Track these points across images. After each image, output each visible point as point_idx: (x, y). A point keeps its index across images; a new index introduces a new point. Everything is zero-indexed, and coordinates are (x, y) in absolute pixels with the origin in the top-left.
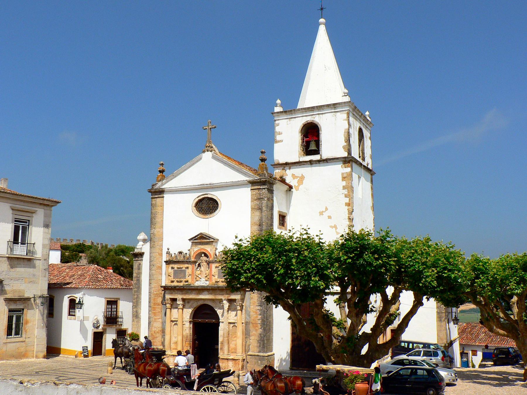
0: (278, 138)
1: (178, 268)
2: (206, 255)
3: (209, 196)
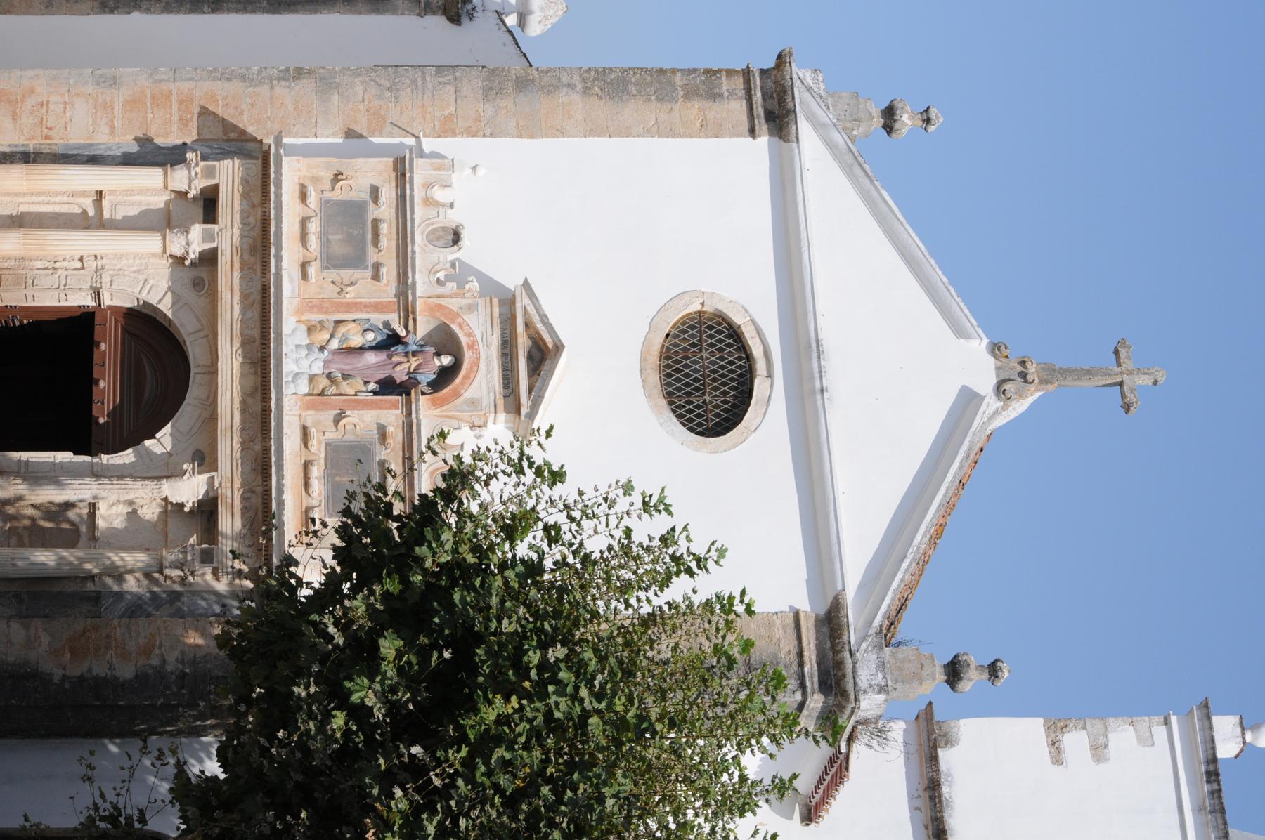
0: (1076, 741)
1: (376, 222)
3: (760, 387)
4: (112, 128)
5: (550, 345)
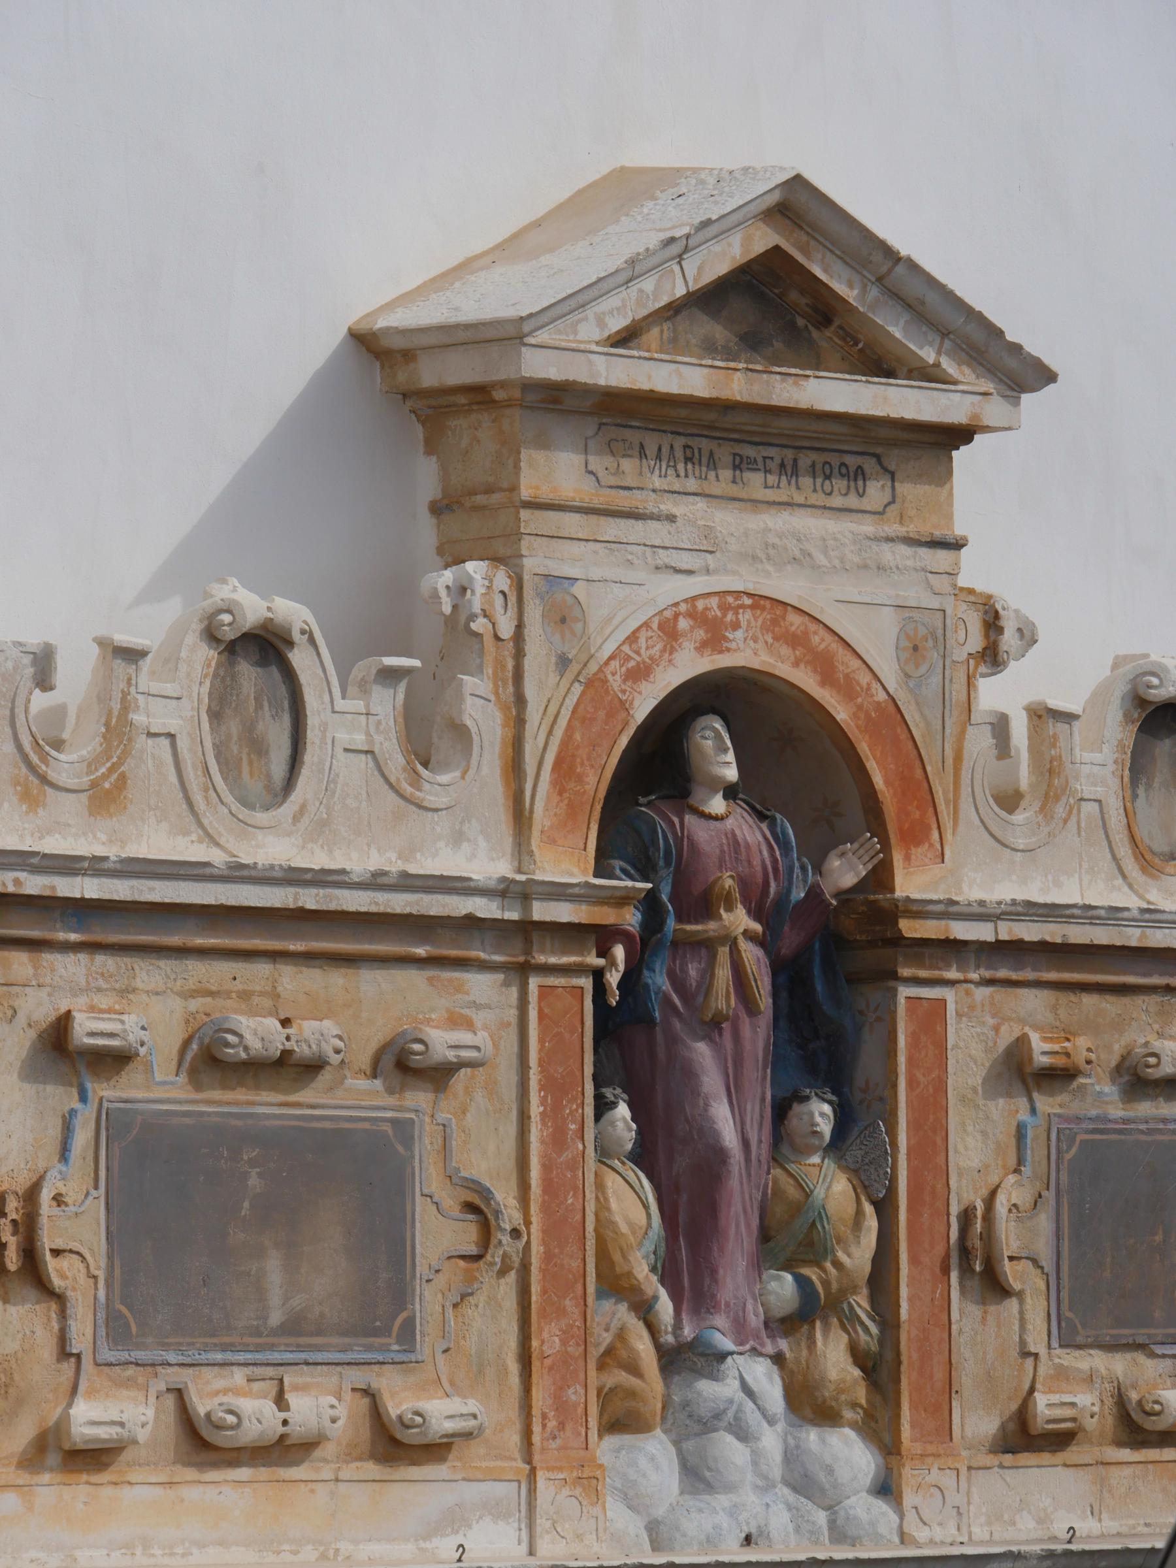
5: (764, 239)
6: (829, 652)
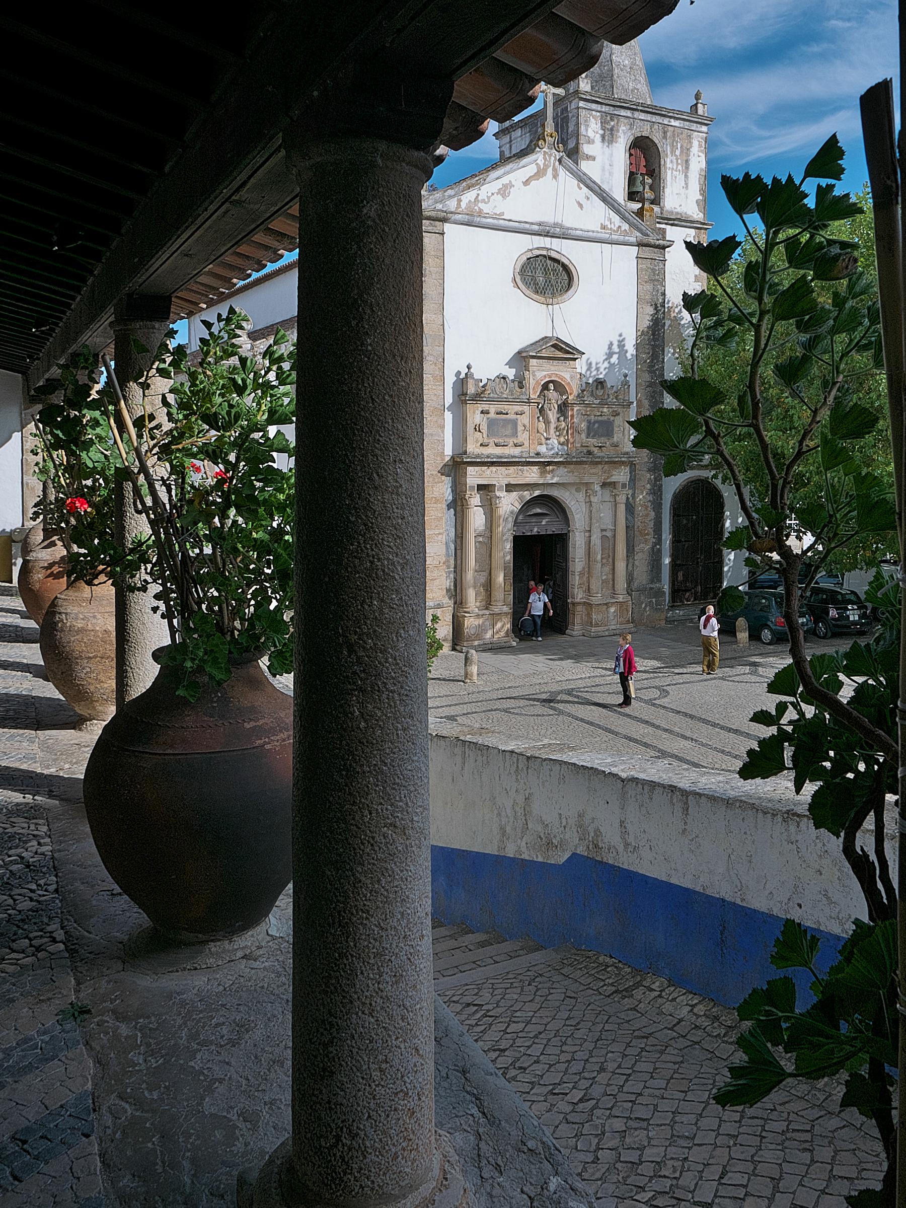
2: (559, 387)
4: (439, 534)
6: (563, 378)
